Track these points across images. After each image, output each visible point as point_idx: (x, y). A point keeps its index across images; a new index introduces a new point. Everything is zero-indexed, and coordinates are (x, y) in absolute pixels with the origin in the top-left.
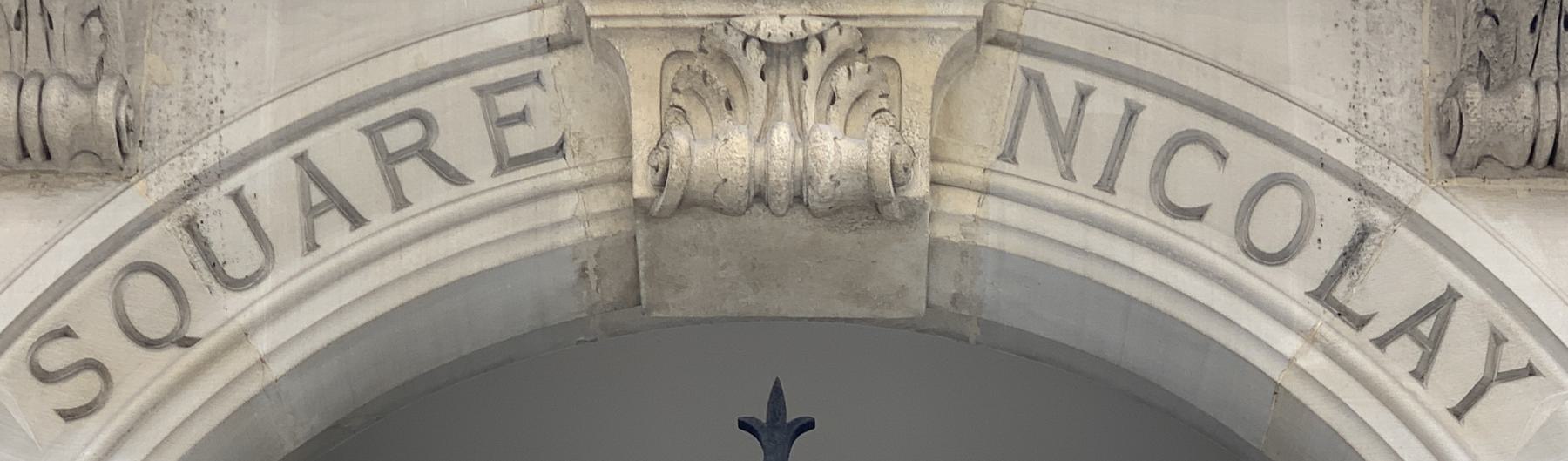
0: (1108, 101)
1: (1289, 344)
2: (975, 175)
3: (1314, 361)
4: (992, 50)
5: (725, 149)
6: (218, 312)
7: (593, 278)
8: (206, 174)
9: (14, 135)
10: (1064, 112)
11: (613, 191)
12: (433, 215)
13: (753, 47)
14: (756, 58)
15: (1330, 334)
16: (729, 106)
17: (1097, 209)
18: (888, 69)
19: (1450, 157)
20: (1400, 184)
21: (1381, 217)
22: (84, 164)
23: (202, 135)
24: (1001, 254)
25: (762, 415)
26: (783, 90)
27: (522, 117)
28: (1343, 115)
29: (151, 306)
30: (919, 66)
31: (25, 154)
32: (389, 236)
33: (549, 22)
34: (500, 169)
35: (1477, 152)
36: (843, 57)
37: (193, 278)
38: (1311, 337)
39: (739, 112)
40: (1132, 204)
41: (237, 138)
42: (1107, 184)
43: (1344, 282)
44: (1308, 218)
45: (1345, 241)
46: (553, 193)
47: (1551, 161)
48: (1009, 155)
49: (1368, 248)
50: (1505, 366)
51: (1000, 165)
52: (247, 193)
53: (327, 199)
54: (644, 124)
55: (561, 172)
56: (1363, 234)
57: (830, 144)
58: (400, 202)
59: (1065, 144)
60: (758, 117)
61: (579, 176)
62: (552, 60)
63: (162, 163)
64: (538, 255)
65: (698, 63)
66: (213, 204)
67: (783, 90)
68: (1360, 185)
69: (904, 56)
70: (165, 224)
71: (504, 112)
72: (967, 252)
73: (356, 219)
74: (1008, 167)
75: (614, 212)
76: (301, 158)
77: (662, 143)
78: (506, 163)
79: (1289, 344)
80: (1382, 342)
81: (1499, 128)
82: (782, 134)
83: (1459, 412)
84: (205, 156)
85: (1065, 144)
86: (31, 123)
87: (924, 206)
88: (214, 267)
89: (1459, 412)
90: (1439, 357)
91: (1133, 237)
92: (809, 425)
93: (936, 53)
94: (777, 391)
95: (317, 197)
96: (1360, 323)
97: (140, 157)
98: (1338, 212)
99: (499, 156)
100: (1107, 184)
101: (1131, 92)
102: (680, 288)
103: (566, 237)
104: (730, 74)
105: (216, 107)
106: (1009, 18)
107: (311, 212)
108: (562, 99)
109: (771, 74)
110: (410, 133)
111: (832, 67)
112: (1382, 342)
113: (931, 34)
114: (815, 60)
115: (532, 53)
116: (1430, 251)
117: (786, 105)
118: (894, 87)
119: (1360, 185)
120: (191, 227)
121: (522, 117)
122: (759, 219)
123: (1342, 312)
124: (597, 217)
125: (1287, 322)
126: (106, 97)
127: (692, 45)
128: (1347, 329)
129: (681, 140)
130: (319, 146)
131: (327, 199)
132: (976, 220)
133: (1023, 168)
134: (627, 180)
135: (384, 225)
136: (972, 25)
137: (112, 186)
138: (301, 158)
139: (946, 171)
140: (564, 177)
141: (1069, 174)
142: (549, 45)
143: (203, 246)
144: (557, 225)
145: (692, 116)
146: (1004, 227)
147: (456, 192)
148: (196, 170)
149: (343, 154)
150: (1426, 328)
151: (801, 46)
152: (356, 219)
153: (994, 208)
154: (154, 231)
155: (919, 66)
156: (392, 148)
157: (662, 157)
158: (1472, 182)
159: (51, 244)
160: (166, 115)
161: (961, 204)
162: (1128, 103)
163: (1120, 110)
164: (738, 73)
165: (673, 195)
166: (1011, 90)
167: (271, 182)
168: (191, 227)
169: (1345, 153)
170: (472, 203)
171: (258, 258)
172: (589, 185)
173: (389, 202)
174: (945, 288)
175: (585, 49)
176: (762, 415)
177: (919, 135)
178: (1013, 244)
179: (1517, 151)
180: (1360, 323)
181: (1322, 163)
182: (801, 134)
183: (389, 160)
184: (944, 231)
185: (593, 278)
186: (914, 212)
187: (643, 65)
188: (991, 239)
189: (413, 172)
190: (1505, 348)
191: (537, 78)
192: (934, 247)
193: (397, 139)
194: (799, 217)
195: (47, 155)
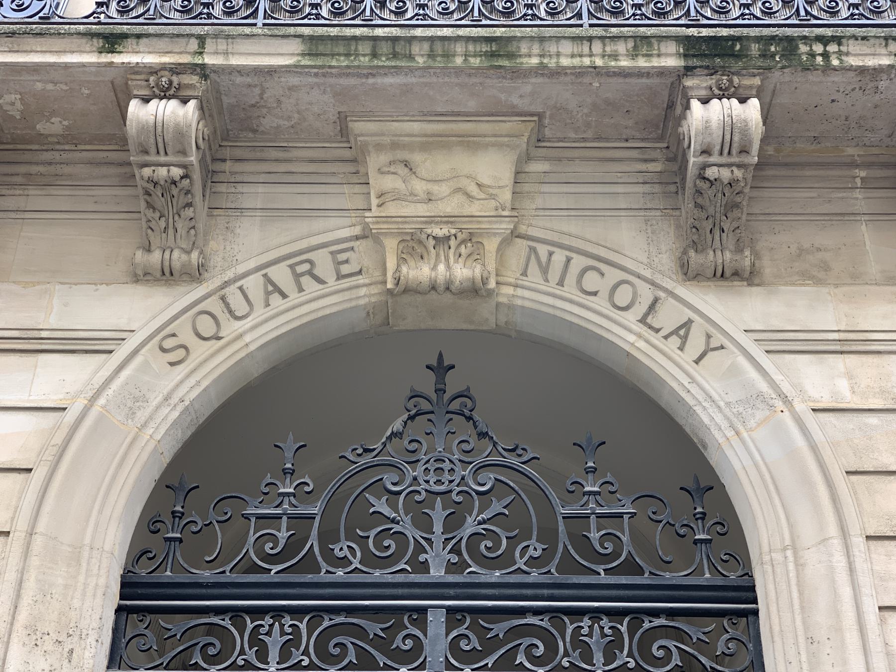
0: (559, 257)
1: (631, 338)
2: (512, 280)
3: (641, 344)
4: (517, 239)
5: (420, 272)
6: (231, 327)
7: (372, 316)
8: (230, 281)
9: (160, 266)
10: (544, 259)
11: (379, 286)
12: (313, 294)
13: (431, 239)
14: (432, 242)
15: (646, 335)
16: (422, 258)
17: (558, 292)
18: (480, 246)
19: (686, 274)
20: (668, 284)
21: (662, 294)
22: (185, 277)
23: (229, 268)
24: (523, 307)
25: (434, 363)
26: (442, 253)
27: (347, 261)
28: (645, 261)
29: (206, 326)
30: (491, 245)
31: (163, 274)
32: (296, 301)
33: (357, 230)
34: (338, 279)
35: (695, 273)
36: (463, 242)
37: (223, 316)
38: (640, 336)
39: (426, 261)
40: (570, 290)
41: (241, 269)
42: (561, 283)
43: (650, 317)
44: (635, 295)
45: (650, 303)
46: (358, 287)
47: (722, 276)
48: (524, 274)
49: (658, 305)
50: (712, 346)
51: (521, 277)
52: (244, 287)
53: (273, 289)
54: (391, 264)
55: (361, 280)
56: (656, 300)
57: (459, 270)
58: (301, 290)
59: (545, 270)
60: (433, 262)
61: (367, 281)
62: (358, 243)
63: (214, 277)
64: (351, 308)
65: (411, 244)
66: (232, 292)
67: (442, 253)
68: (653, 283)
69: (485, 242)
70: (213, 297)
71: (340, 260)
72: (511, 307)
73: (284, 296)
74: (524, 278)
75: (379, 293)
76: (265, 275)
77: (398, 269)
78: (340, 277)
79: (631, 338)
80: (666, 337)
81: (702, 265)
82: (441, 267)
83: (697, 362)
84: (230, 275)
85: (545, 270)
86: (167, 264)
87: (494, 291)
88: (231, 312)
89: (697, 362)
90: (687, 343)
91: (571, 301)
92: (453, 367)
93: (496, 241)
94: (441, 355)
95: (270, 288)
96: (657, 331)
97: (206, 275)
98: (646, 294)
99: (338, 274)
100: (561, 283)
101: (568, 253)
102: (404, 319)
103: (362, 302)
104: (423, 249)
105: (235, 259)
106: (523, 229)
107: (268, 294)
108: (361, 255)
109: (437, 247)
110: (306, 267)
111: (459, 245)
112: (666, 337)
113: (495, 234)
114: (453, 242)
115: (351, 241)
116: (681, 306)
117: (443, 258)
118: (482, 252)
119: (653, 283)
120: (223, 299)
121: (347, 261)
122: (433, 295)
123: (650, 327)
124: (373, 295)
125: (630, 331)
126: (195, 255)
127: (408, 238)
128: (653, 333)
129: (404, 269)
130: (272, 272)
131: (273, 289)
132: (513, 296)
133: (529, 279)
134: (385, 282)
135: (294, 297)
136: (509, 231)
137: (195, 285)
138: (265, 275)
139: (501, 279)
140: (361, 281)
141: (547, 280)
142: (357, 238)
143: (227, 305)
144: (358, 298)
145: (409, 261)
146: (523, 298)
147: (321, 286)
148: (226, 279)
149: (281, 275)
150: (682, 332)
151: (448, 238)
152: (284, 296)
153: (520, 292)
154: (209, 300)
155: (491, 245)
156: (298, 272)
157: (397, 275)
158: (695, 283)
159: (170, 305)
160: (216, 261)
161: (508, 290)
162: (567, 257)
163: (565, 259)
164: (425, 247)
165: (402, 287)
166: (524, 253)
167: (254, 284)
168: (223, 299)
169: (647, 273)
170: (327, 290)
171: (248, 309)
172: (370, 284)
173: (297, 290)
174: (502, 319)
175: (370, 239)
176: (434, 363)
177: (491, 266)
178: (527, 304)
179: (710, 273)
180: (657, 331)
181: (639, 276)
182: (448, 267)
183: (297, 276)
184: (501, 299)
185: (372, 316)
186: (490, 293)
187: (391, 245)
188: (519, 302)
189: (306, 280)
190: (712, 339)
191: (352, 249)
192: (498, 305)
193: (300, 269)
194: (448, 295)
195: (172, 274)
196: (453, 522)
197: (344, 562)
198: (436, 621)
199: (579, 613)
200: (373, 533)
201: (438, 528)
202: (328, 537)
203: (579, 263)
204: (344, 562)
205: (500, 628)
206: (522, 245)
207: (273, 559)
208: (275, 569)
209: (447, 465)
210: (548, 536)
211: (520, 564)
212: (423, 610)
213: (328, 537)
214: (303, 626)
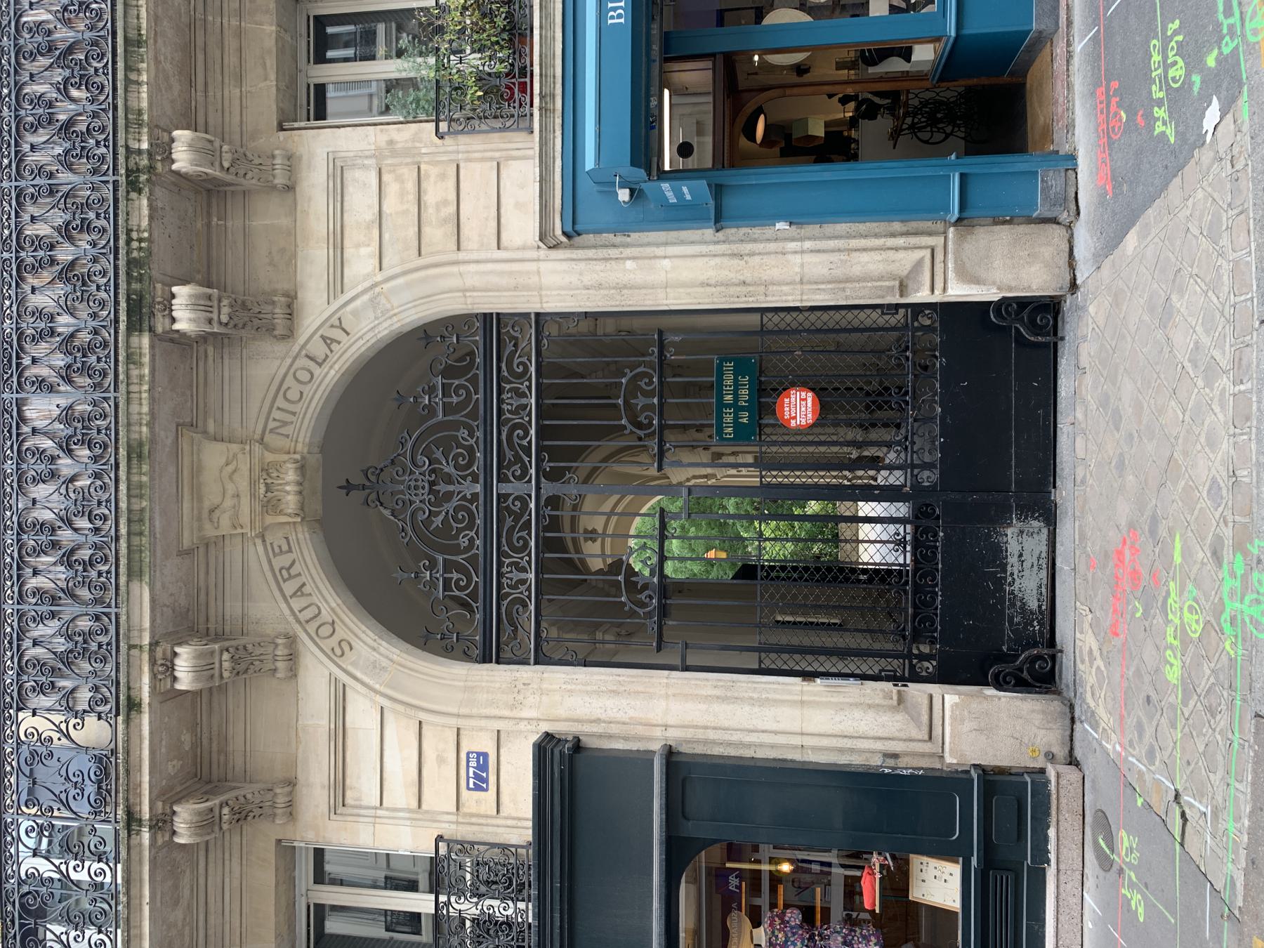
0: (276, 414)
1: (332, 372)
3: (337, 367)
5: (291, 501)
6: (326, 615)
10: (278, 424)
14: (269, 494)
20: (296, 348)
21: (304, 352)
25: (345, 491)
29: (326, 630)
30: (270, 457)
33: (258, 541)
38: (331, 367)
41: (287, 612)
42: (294, 414)
44: (303, 369)
55: (292, 538)
56: (307, 356)
58: (299, 574)
59: (285, 424)
68: (295, 358)
72: (310, 444)
73: (304, 584)
77: (289, 515)
78: (290, 551)
79: (332, 372)
82: (288, 488)
83: (348, 334)
84: (291, 619)
85: (285, 424)
89: (348, 334)
93: (267, 454)
96: (327, 356)
98: (302, 362)
100: (294, 414)
103: (307, 536)
106: (257, 437)
107: (303, 595)
108: (276, 539)
110: (284, 572)
114: (269, 481)
119: (295, 358)
120: (307, 622)
122: (305, 493)
126: (279, 641)
129: (290, 511)
130: (288, 593)
142: (264, 541)
143: (312, 619)
149: (289, 588)
151: (266, 484)
152: (304, 584)
153: (300, 440)
155: (270, 457)
160: (281, 628)
166: (274, 436)
167: (297, 604)
168: (307, 622)
169: (289, 361)
176: (345, 491)
177: (286, 457)
180: (327, 356)
181: (291, 366)
182: (287, 484)
183: (291, 577)
184: (306, 450)
186: (303, 458)
187: (269, 520)
188: (307, 440)
189: (293, 572)
196: (449, 480)
197: (471, 540)
198: (506, 488)
199: (500, 412)
200: (455, 525)
201: (451, 488)
202: (457, 550)
203: (280, 402)
204: (471, 540)
205: (509, 454)
206: (267, 438)
207: (469, 580)
208: (475, 578)
209: (413, 483)
210: (456, 426)
211: (472, 442)
212: (498, 495)
213: (457, 550)
214: (507, 561)
